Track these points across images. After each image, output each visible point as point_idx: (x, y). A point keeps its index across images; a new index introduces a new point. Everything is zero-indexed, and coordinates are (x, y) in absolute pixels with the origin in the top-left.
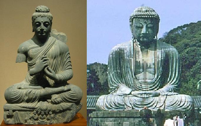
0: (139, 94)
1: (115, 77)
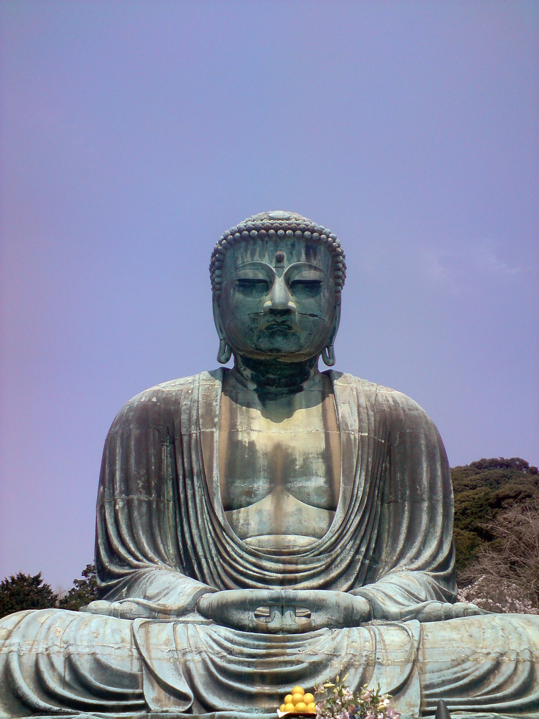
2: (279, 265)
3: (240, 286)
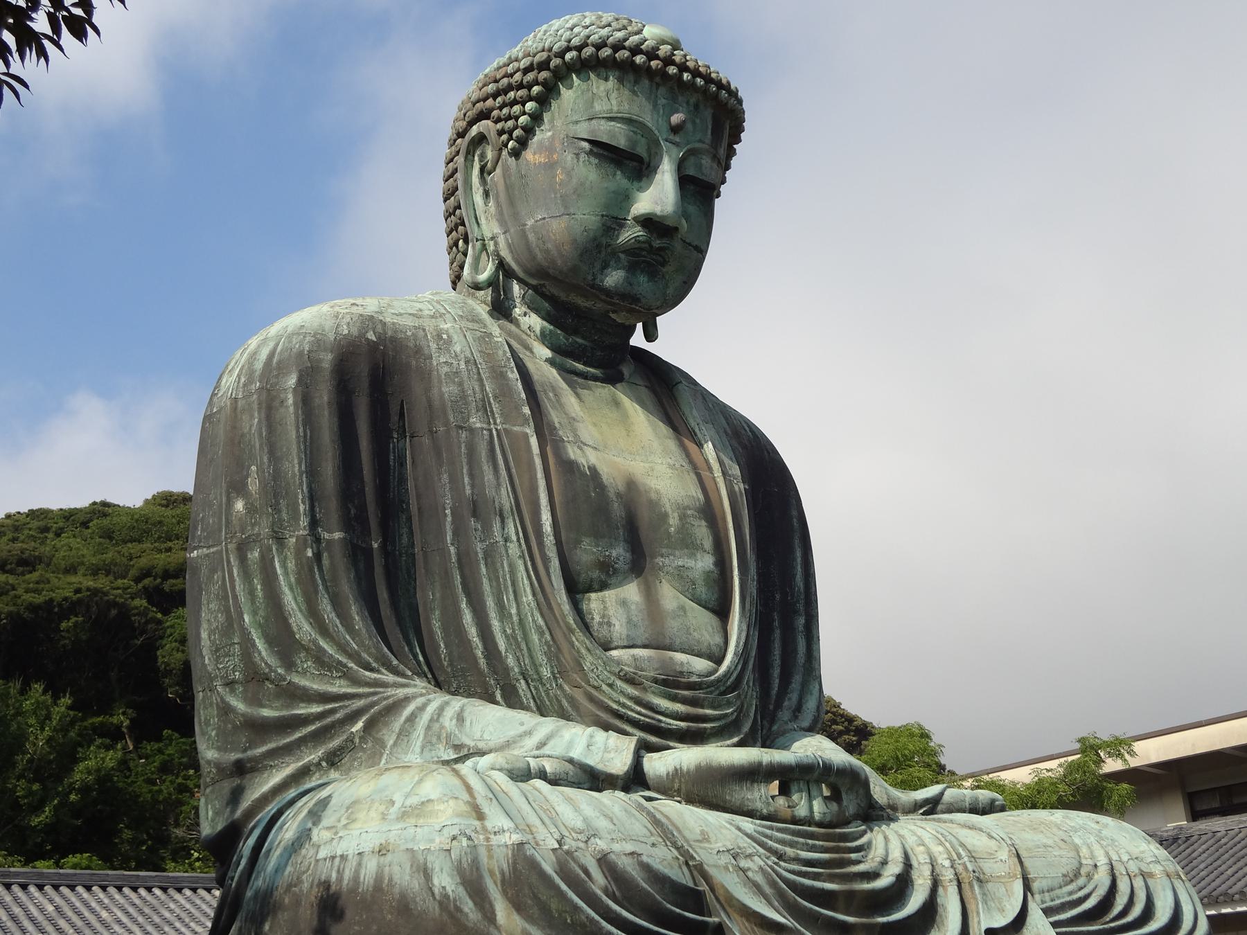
0: (753, 774)
2: (671, 137)
3: (590, 153)
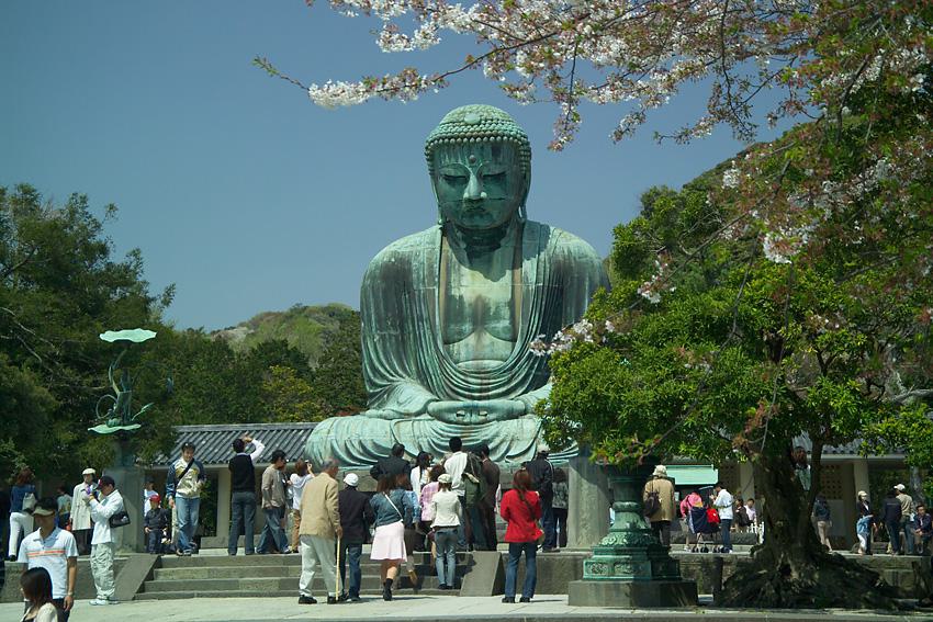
0: (451, 410)
1: (382, 357)
